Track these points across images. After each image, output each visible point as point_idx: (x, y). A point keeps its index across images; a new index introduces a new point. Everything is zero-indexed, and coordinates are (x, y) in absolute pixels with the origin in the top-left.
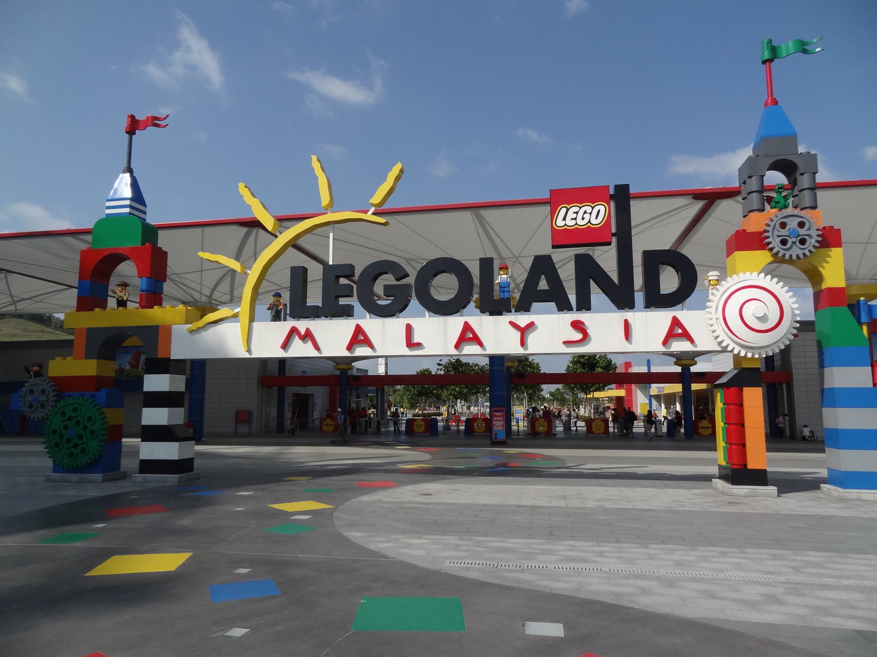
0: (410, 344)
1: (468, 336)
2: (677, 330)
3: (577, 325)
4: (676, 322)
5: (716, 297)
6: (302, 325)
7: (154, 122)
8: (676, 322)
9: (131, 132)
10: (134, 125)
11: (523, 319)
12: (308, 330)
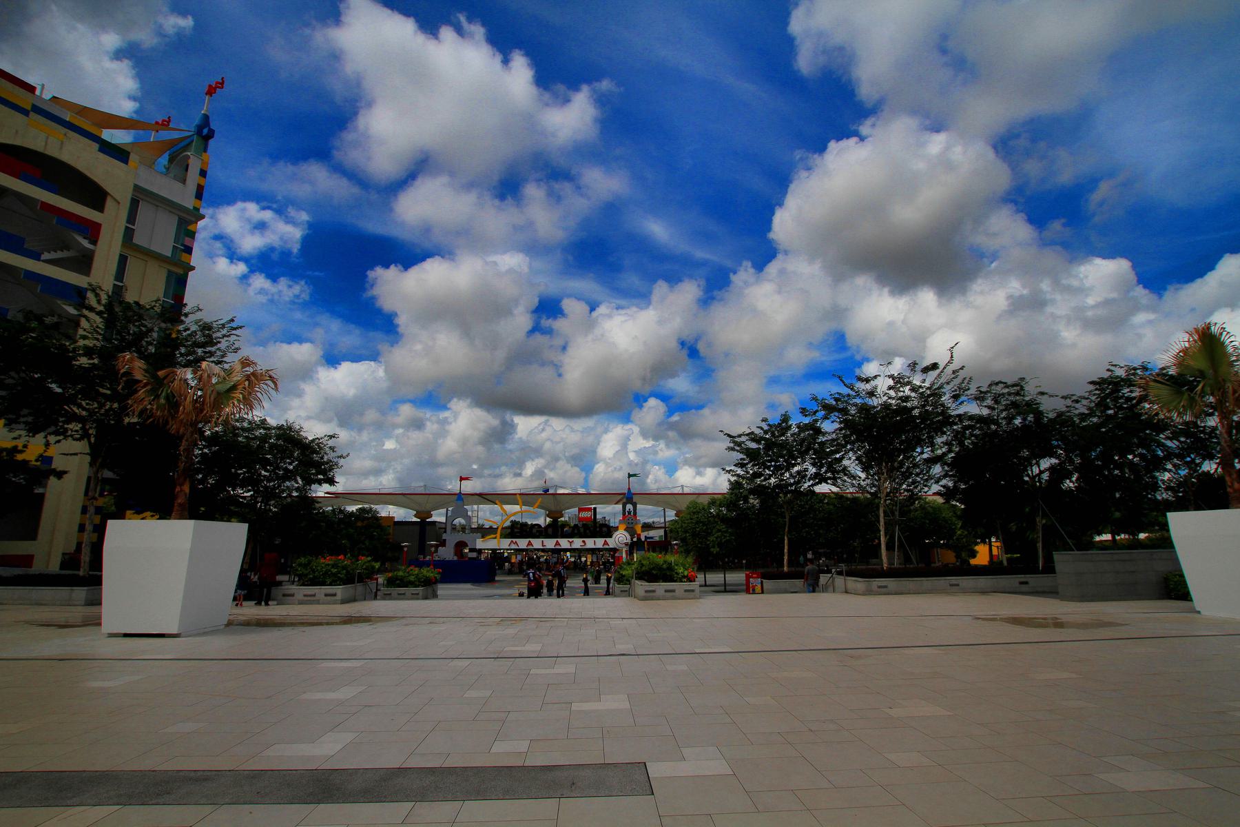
0: (543, 546)
1: (557, 543)
2: (606, 543)
3: (584, 541)
4: (605, 541)
5: (614, 536)
6: (514, 540)
7: (467, 479)
8: (605, 541)
9: (461, 481)
10: (462, 479)
11: (571, 540)
12: (516, 542)
